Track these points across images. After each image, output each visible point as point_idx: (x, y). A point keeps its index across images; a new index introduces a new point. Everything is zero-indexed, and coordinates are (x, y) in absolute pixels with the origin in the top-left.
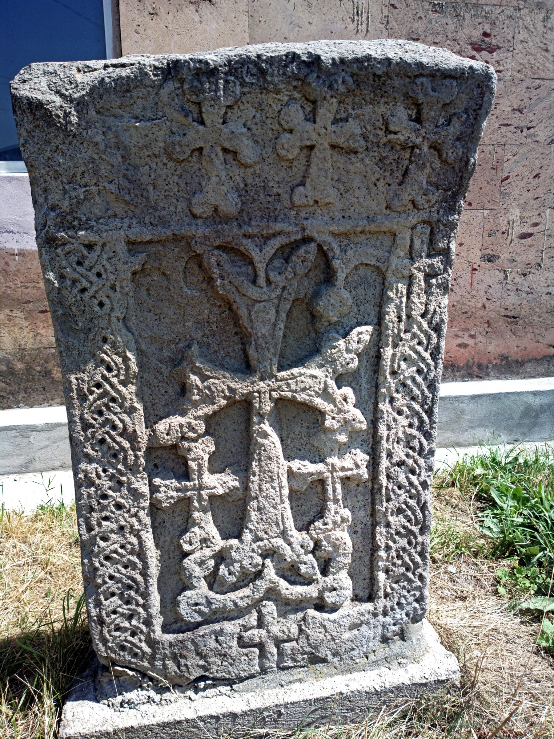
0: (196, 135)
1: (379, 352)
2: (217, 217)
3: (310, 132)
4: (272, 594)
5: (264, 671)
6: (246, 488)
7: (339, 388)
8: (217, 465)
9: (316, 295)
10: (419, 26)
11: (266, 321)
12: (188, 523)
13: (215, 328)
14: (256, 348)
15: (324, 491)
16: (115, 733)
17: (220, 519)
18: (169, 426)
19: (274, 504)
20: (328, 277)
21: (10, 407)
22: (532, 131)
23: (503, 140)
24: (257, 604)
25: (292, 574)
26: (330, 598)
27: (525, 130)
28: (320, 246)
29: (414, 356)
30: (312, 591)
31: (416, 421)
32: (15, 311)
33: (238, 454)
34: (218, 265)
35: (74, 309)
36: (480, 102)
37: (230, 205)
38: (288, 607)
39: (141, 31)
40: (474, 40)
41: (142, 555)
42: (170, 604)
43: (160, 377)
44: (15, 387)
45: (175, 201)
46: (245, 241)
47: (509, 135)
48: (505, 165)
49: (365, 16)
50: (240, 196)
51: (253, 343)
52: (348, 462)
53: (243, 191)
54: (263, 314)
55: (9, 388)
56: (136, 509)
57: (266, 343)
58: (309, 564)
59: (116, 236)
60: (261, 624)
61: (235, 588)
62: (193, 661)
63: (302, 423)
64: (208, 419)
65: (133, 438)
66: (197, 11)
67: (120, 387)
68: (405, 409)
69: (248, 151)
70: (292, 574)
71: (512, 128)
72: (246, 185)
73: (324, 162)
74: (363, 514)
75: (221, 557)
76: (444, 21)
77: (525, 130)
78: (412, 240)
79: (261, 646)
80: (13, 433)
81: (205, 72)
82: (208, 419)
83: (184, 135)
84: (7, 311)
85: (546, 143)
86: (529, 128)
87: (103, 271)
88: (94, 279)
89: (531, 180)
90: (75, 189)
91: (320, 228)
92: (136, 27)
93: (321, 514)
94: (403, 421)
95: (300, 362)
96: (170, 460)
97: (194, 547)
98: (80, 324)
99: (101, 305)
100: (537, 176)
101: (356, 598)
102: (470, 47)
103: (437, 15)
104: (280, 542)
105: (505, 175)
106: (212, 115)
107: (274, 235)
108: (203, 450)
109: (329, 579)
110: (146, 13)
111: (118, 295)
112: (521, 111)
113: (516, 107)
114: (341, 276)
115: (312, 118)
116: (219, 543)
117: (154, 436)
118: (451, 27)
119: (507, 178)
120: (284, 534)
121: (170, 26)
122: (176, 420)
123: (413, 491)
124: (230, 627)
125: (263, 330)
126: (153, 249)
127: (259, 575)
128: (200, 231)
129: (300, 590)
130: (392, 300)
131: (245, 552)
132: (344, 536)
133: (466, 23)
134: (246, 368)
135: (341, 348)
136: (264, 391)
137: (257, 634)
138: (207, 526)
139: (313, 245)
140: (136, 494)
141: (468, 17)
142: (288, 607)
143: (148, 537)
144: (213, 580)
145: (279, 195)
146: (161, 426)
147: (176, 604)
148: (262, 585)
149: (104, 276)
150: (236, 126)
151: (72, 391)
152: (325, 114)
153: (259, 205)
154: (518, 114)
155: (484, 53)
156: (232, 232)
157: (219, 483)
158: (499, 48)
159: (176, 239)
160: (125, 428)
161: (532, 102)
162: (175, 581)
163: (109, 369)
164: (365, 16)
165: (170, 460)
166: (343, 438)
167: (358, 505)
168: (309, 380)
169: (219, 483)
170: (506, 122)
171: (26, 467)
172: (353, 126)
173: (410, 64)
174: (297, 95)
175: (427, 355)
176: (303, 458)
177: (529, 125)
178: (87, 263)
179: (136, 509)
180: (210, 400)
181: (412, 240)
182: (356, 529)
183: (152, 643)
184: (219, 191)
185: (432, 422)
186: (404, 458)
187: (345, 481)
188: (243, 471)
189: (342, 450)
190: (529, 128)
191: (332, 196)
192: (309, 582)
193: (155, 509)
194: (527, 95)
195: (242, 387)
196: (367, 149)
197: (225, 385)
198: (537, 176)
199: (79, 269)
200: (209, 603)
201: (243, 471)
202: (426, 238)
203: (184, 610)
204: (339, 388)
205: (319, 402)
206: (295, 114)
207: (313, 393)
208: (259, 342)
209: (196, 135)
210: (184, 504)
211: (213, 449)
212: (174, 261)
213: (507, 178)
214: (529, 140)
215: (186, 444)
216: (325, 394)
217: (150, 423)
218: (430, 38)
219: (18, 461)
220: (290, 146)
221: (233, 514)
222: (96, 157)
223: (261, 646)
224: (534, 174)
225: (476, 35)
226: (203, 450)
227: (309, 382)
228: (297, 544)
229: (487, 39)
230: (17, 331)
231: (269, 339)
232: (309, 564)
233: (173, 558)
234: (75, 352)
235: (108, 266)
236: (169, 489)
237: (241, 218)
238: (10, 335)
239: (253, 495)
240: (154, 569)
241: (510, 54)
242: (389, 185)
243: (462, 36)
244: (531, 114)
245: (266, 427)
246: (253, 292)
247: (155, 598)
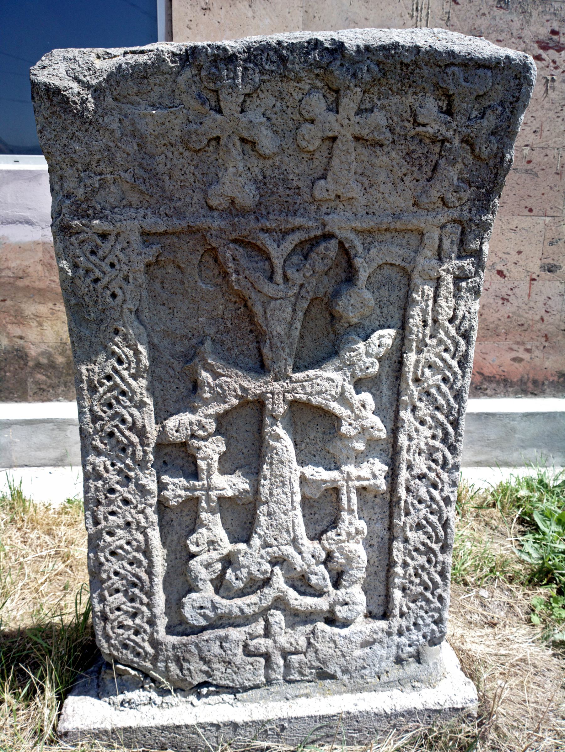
0: (213, 124)
1: (402, 357)
2: (234, 209)
3: (332, 123)
4: (280, 603)
5: (269, 682)
6: (256, 492)
7: (358, 393)
8: (227, 465)
9: (337, 294)
10: (483, 23)
11: (282, 320)
12: (195, 524)
13: (229, 325)
14: (271, 348)
15: (339, 500)
16: (113, 732)
17: (229, 522)
18: (179, 423)
19: (284, 511)
20: (350, 276)
21: (49, 400)
24: (264, 613)
25: (302, 584)
26: (341, 612)
28: (341, 244)
29: (440, 363)
30: (322, 604)
31: (440, 433)
32: (58, 305)
33: (249, 456)
34: (234, 259)
35: (86, 299)
36: (517, 94)
37: (247, 196)
38: (297, 618)
39: (193, 25)
40: (541, 37)
41: (147, 553)
42: (174, 605)
43: (172, 373)
44: (55, 381)
45: (191, 192)
46: (262, 236)
49: (424, 12)
50: (258, 188)
51: (268, 341)
52: (364, 471)
53: (261, 183)
54: (278, 312)
55: (49, 381)
56: (143, 506)
57: (281, 342)
58: (320, 576)
59: (130, 226)
60: (267, 633)
61: (242, 593)
62: (196, 665)
63: (317, 427)
64: (219, 418)
65: (142, 433)
66: (250, 6)
67: (131, 381)
68: (428, 419)
69: (267, 142)
70: (302, 584)
72: (265, 177)
73: (347, 156)
74: (380, 528)
75: (229, 561)
76: (509, 17)
78: (441, 240)
79: (267, 656)
80: (51, 426)
82: (219, 418)
83: (201, 123)
84: (51, 305)
87: (116, 262)
88: (108, 269)
90: (90, 177)
91: (341, 224)
92: (188, 22)
93: (334, 524)
94: (426, 432)
95: (317, 363)
96: (178, 457)
97: (200, 548)
98: (92, 315)
99: (114, 296)
101: (370, 615)
102: (536, 45)
103: (503, 11)
104: (289, 550)
106: (231, 104)
107: (293, 230)
108: (212, 449)
109: (341, 593)
110: (199, 8)
111: (131, 287)
114: (363, 275)
115: (334, 108)
116: (227, 547)
117: (163, 433)
118: (517, 24)
120: (294, 542)
121: (222, 22)
122: (186, 417)
123: (434, 506)
124: (236, 634)
125: (279, 329)
126: (167, 241)
127: (267, 582)
128: (216, 223)
129: (309, 602)
130: (417, 303)
131: (253, 557)
132: (359, 550)
133: (533, 20)
134: (261, 368)
135: (360, 351)
136: (277, 392)
137: (263, 644)
138: (214, 528)
139: (334, 242)
140: (143, 490)
141: (535, 13)
142: (297, 618)
143: (155, 535)
144: (219, 584)
145: (299, 188)
146: (171, 423)
147: (181, 606)
148: (270, 593)
149: (117, 267)
150: (255, 115)
151: (82, 382)
152: (349, 103)
153: (277, 196)
155: (551, 52)
156: (248, 226)
157: (230, 484)
159: (191, 230)
160: (134, 423)
162: (181, 582)
163: (120, 362)
164: (424, 12)
165: (178, 457)
166: (360, 446)
167: (375, 517)
168: (326, 383)
169: (230, 484)
171: (62, 460)
172: (379, 118)
173: (440, 52)
174: (319, 84)
175: (454, 363)
176: (317, 465)
178: (100, 253)
179: (143, 506)
180: (221, 398)
181: (441, 240)
182: (372, 542)
183: (155, 643)
184: (236, 182)
185: (458, 434)
186: (425, 470)
187: (362, 491)
188: (254, 473)
189: (359, 458)
191: (355, 190)
192: (320, 593)
193: (162, 506)
195: (255, 387)
196: (393, 142)
197: (239, 383)
199: (93, 258)
200: (214, 607)
201: (254, 473)
202: (456, 237)
203: (188, 612)
204: (358, 393)
205: (336, 407)
206: (317, 104)
207: (329, 397)
208: (273, 341)
209: (213, 124)
210: (193, 503)
211: (223, 449)
212: (188, 254)
215: (195, 443)
216: (342, 399)
217: (160, 418)
218: (493, 36)
219: (54, 454)
220: (311, 137)
221: (242, 517)
222: (112, 144)
223: (267, 656)
225: (544, 32)
226: (212, 449)
227: (326, 385)
228: (308, 554)
229: (555, 37)
230: (59, 325)
231: (285, 338)
232: (320, 576)
233: (181, 558)
234: (87, 343)
235: (121, 256)
236: (177, 487)
237: (258, 211)
238: (52, 328)
239: (264, 499)
240: (160, 568)
242: (417, 181)
243: (528, 34)
245: (279, 430)
246: (269, 289)
247: (160, 599)
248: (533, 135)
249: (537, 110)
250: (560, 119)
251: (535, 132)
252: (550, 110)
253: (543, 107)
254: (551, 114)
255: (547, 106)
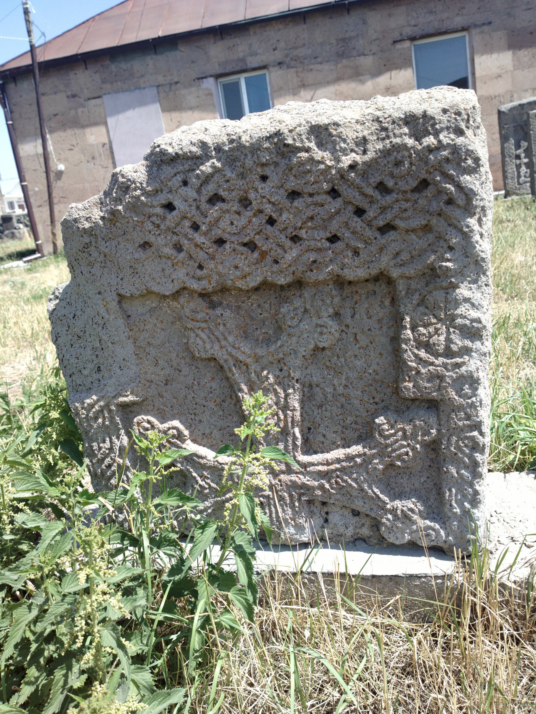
8: (525, 157)
18: (518, 152)
42: (518, 181)
59: (512, 125)
81: (524, 104)
96: (518, 157)
108: (523, 155)
144: (525, 176)
157: (526, 160)
162: (519, 176)
165: (518, 157)
169: (526, 160)
226: (523, 155)
233: (519, 173)
236: (518, 162)
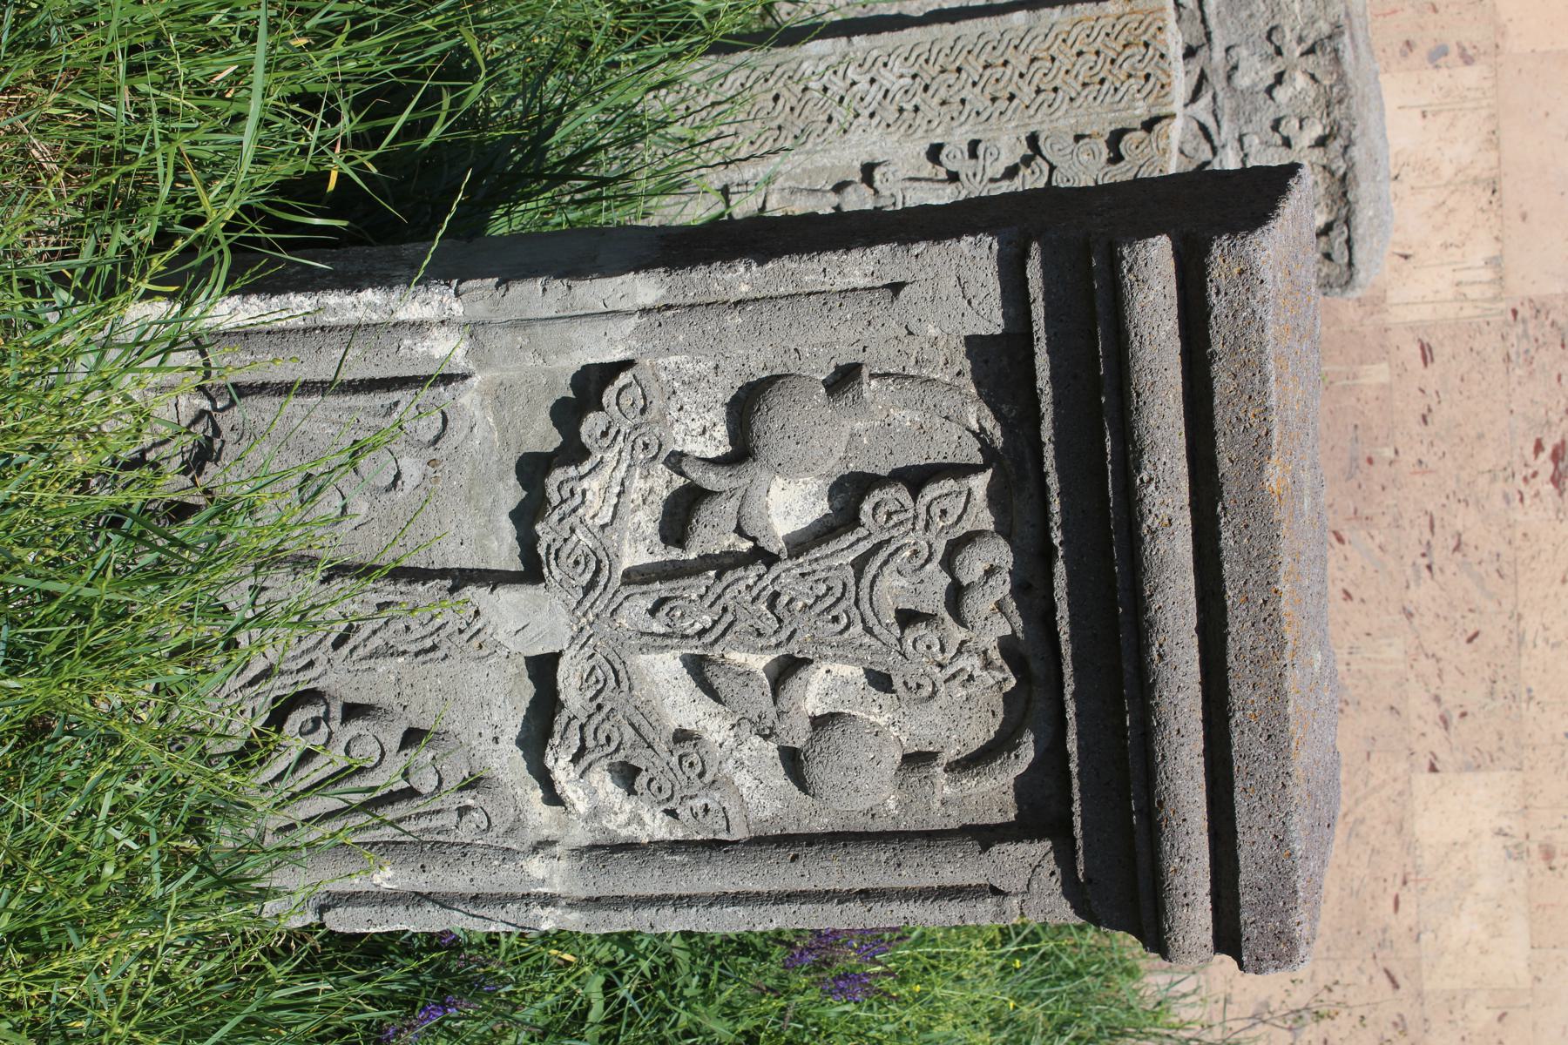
22: (1425, 573)
23: (1405, 523)
27: (1426, 561)
47: (1415, 533)
48: (1363, 533)
71: (1427, 535)
77: (1426, 561)
85: (1407, 604)
86: (1429, 567)
89: (1340, 585)
100: (1348, 595)
102: (1558, 440)
105: (1346, 535)
112: (1457, 548)
113: (1464, 538)
119: (1340, 540)
154: (1452, 543)
155: (1550, 467)
158: (1561, 494)
161: (1476, 568)
170: (1437, 523)
177: (1435, 568)
190: (1429, 567)
194: (1485, 556)
198: (1348, 595)
213: (1340, 540)
214: (1409, 571)
224: (1351, 590)
241: (1552, 514)
244: (1453, 568)
248: (1414, 460)
249: (1455, 459)
250: (1444, 501)
251: (1420, 462)
252: (1458, 481)
253: (1461, 468)
254: (1451, 485)
255: (1464, 475)
